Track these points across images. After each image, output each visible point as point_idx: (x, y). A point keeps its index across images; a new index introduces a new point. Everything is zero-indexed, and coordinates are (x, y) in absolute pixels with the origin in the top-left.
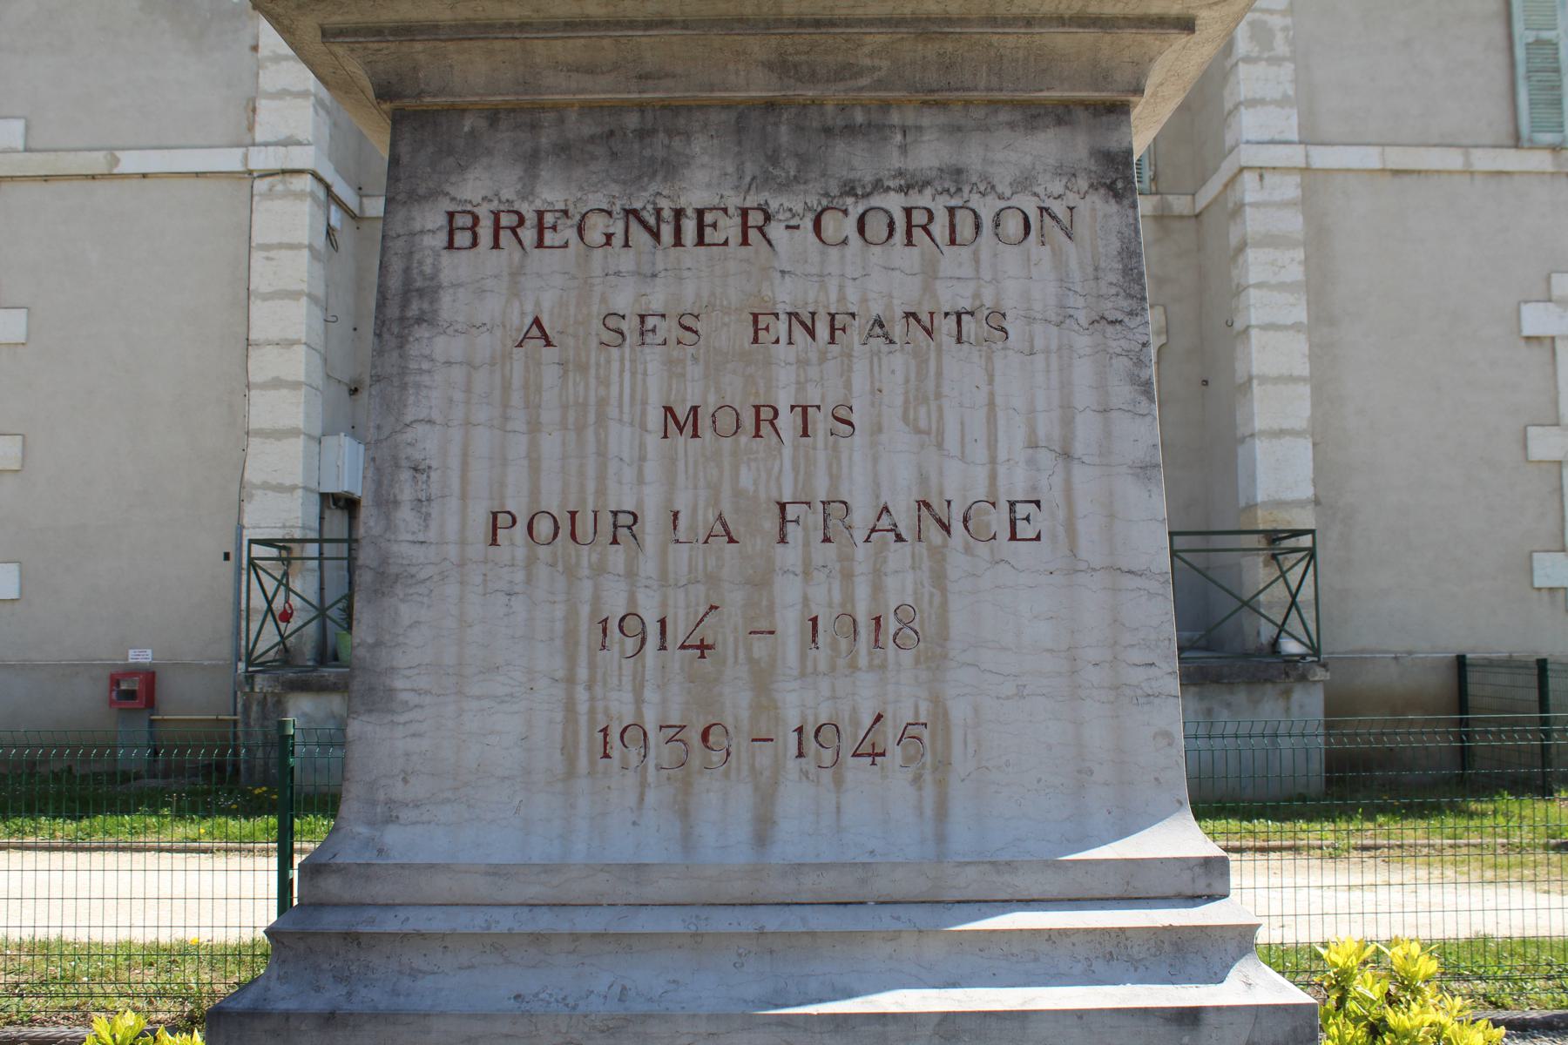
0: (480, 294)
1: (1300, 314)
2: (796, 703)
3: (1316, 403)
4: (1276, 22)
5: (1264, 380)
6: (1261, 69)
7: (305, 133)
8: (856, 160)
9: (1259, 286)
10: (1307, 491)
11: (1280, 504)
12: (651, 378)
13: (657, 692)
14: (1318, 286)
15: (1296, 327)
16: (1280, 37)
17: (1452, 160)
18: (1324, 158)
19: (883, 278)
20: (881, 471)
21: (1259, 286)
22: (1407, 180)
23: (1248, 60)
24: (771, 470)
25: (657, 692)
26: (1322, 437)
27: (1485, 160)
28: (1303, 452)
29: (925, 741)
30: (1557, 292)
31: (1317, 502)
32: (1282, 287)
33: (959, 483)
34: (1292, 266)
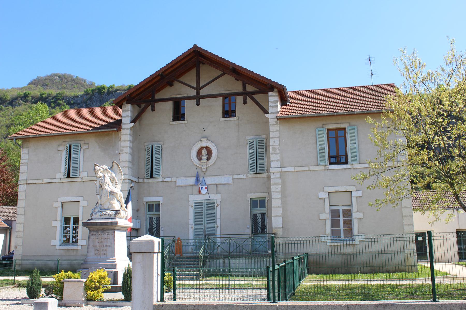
0: (92, 237)
1: (280, 196)
2: (102, 253)
3: (282, 211)
4: (277, 147)
5: (274, 207)
6: (274, 155)
7: (127, 173)
8: (105, 232)
9: (273, 192)
10: (281, 226)
11: (276, 228)
12: (97, 240)
13: (97, 252)
14: (283, 192)
15: (279, 198)
16: (277, 149)
17: (307, 168)
18: (284, 170)
19: (106, 236)
20: (105, 244)
21: (273, 192)
22: (299, 172)
23: (272, 154)
24: (102, 244)
25: (97, 252)
26: (284, 217)
27: (312, 168)
28: (280, 219)
29: (106, 254)
30: (325, 190)
31: (283, 227)
32: (277, 192)
33: (108, 245)
34: (279, 188)
